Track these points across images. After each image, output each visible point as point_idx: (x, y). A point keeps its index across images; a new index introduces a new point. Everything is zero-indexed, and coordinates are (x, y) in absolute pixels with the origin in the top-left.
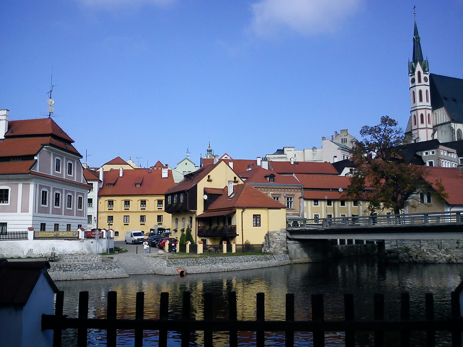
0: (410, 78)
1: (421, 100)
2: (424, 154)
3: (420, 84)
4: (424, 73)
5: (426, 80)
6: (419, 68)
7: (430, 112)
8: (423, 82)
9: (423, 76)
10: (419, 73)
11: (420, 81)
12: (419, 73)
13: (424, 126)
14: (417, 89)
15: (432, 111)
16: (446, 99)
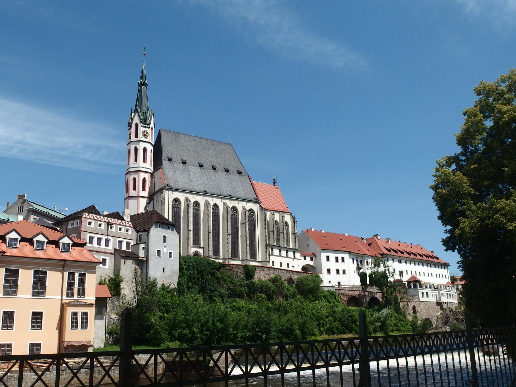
0: (129, 132)
1: (136, 160)
2: (70, 226)
3: (136, 139)
4: (143, 126)
5: (145, 135)
6: (136, 120)
7: (147, 177)
8: (141, 137)
9: (141, 129)
10: (137, 126)
11: (137, 136)
12: (137, 126)
13: (135, 194)
14: (132, 147)
15: (152, 174)
16: (170, 160)
